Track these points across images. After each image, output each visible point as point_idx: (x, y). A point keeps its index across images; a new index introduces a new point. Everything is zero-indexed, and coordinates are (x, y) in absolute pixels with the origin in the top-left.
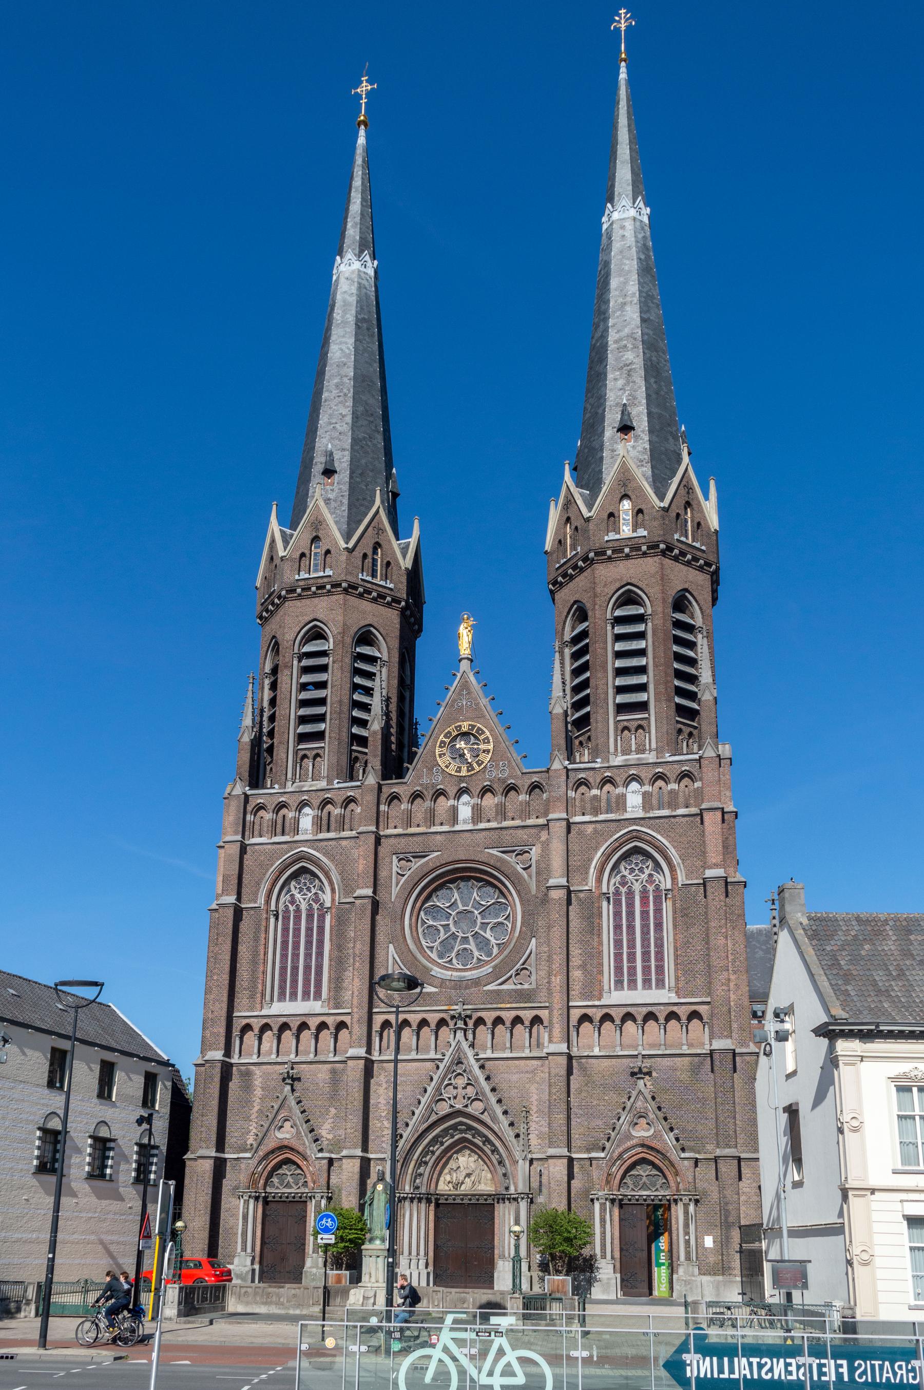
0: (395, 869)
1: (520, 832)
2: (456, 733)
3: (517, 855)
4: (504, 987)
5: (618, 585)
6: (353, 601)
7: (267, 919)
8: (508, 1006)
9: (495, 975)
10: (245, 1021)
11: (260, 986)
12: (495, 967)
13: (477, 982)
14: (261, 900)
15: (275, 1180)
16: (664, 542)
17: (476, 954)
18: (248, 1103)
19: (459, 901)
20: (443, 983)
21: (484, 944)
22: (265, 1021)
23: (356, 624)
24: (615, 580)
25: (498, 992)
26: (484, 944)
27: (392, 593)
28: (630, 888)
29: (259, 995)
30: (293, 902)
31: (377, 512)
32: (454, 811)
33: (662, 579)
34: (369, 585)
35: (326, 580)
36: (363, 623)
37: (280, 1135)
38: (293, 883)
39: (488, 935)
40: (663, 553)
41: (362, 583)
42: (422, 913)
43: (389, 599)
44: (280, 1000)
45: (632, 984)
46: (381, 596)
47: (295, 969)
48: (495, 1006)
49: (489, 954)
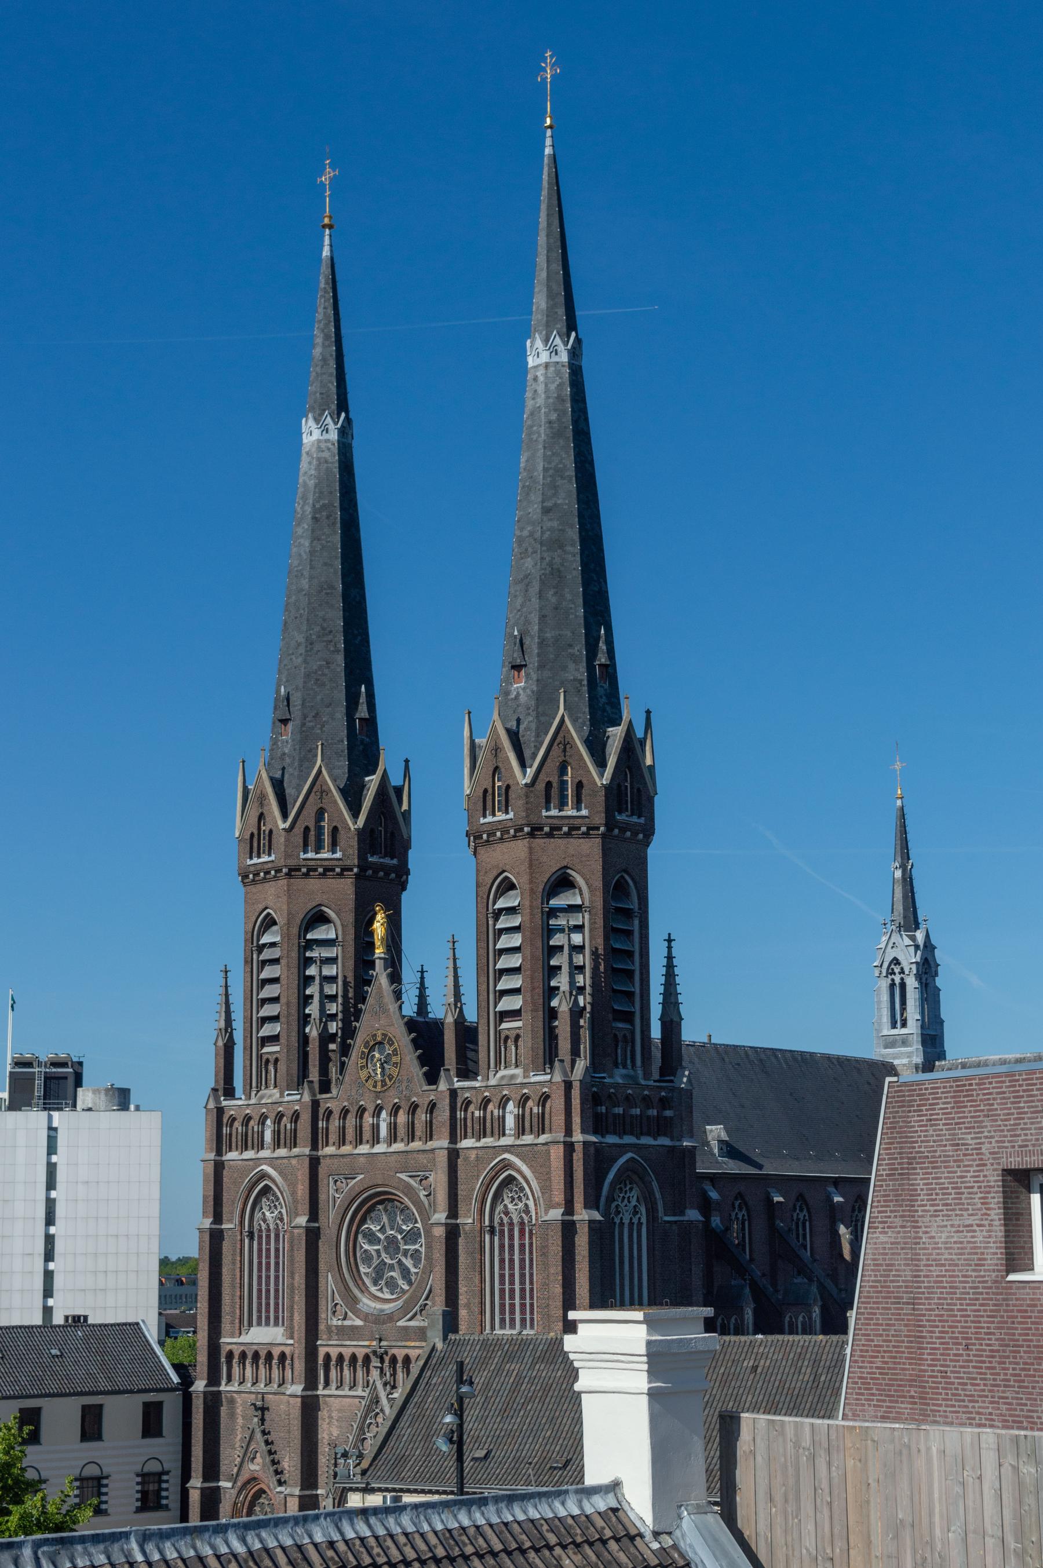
0: (331, 1191)
1: (421, 1156)
2: (372, 1043)
3: (421, 1180)
4: (412, 1323)
5: (495, 873)
6: (298, 883)
7: (242, 1241)
8: (413, 1344)
9: (404, 1310)
10: (229, 1347)
11: (238, 1311)
12: (405, 1302)
13: (391, 1318)
14: (237, 1220)
15: (257, 1509)
16: (528, 825)
17: (400, 1282)
18: (233, 1431)
19: (387, 1225)
20: (365, 1317)
21: (405, 1273)
22: (242, 1348)
23: (303, 908)
24: (497, 866)
25: (406, 1328)
26: (405, 1273)
27: (341, 863)
28: (511, 1218)
29: (237, 1321)
30: (265, 1220)
31: (319, 772)
32: (375, 1128)
33: (531, 866)
34: (312, 863)
35: (270, 865)
36: (314, 904)
37: (252, 1467)
38: (264, 1200)
39: (408, 1263)
40: (531, 835)
41: (304, 863)
42: (360, 1237)
43: (338, 870)
44: (259, 1324)
45: (512, 1326)
46: (327, 870)
47: (268, 1291)
48: (403, 1344)
49: (410, 1283)
